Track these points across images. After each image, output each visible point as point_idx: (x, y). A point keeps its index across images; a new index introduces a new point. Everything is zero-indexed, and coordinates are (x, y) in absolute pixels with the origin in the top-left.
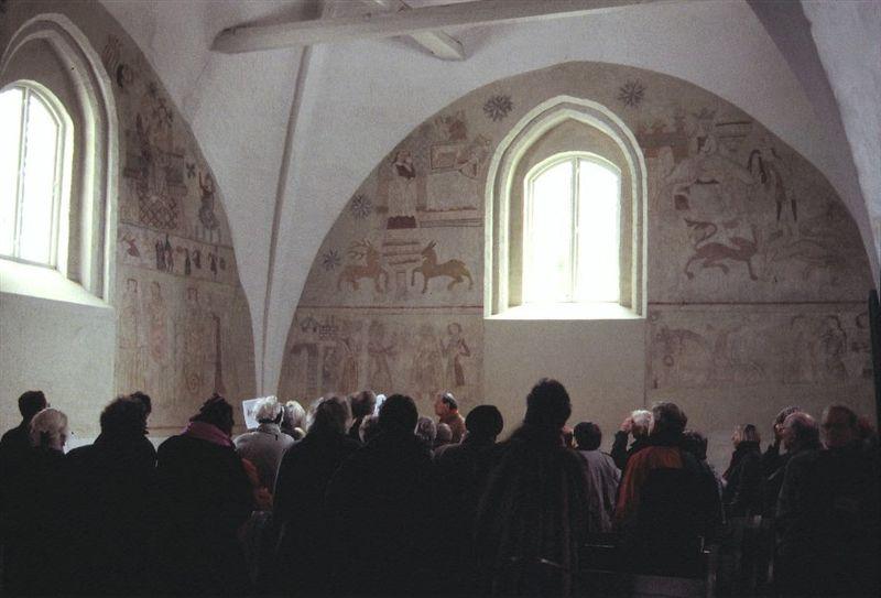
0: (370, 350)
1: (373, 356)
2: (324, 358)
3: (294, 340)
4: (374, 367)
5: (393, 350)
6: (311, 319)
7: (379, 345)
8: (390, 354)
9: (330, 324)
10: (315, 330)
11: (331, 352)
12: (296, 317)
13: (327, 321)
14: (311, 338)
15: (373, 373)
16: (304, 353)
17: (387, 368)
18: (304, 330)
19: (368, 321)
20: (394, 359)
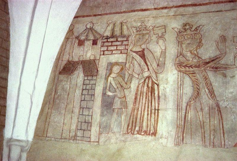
0: (182, 65)
1: (185, 73)
2: (106, 79)
3: (66, 58)
4: (188, 90)
5: (223, 62)
6: (91, 29)
7: (196, 56)
8: (216, 69)
9: (117, 32)
10: (95, 43)
11: (116, 69)
12: (71, 31)
13: (113, 30)
14: (88, 52)
15: (185, 100)
16: (79, 76)
17: (212, 93)
18: (81, 43)
19: (176, 25)
20: (225, 76)
